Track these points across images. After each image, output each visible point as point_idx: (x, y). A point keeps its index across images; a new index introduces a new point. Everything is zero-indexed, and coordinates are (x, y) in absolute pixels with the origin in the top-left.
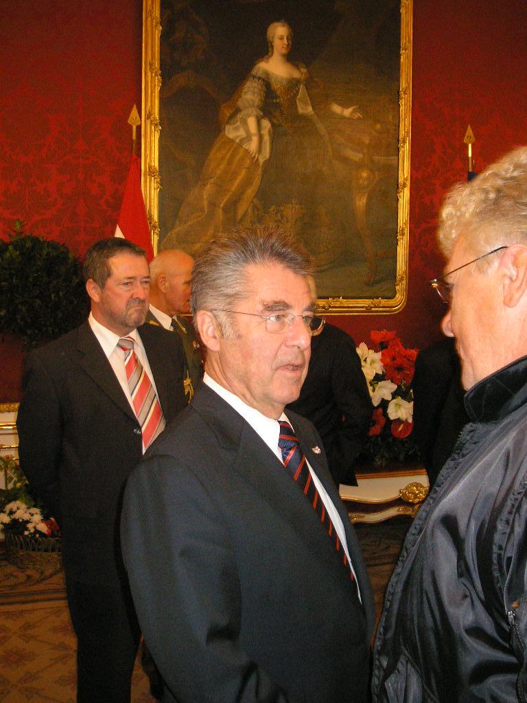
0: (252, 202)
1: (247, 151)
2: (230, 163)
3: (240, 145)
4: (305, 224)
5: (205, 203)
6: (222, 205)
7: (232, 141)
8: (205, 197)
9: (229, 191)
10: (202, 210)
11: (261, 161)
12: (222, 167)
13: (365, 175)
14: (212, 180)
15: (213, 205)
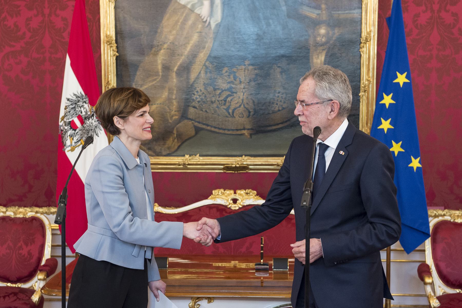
0: (205, 65)
1: (199, 16)
2: (182, 28)
3: (192, 10)
4: (259, 84)
5: (160, 67)
6: (175, 69)
7: (184, 7)
8: (159, 61)
9: (182, 55)
10: (157, 74)
11: (213, 25)
12: (174, 32)
13: (323, 31)
14: (165, 46)
15: (167, 68)
